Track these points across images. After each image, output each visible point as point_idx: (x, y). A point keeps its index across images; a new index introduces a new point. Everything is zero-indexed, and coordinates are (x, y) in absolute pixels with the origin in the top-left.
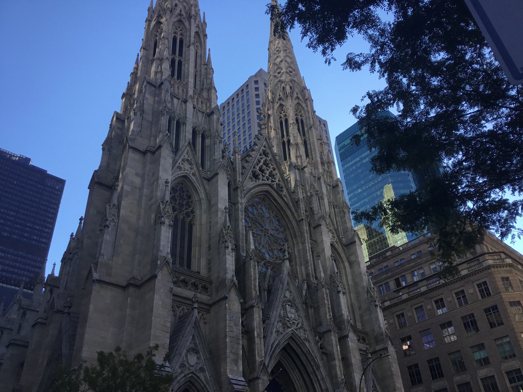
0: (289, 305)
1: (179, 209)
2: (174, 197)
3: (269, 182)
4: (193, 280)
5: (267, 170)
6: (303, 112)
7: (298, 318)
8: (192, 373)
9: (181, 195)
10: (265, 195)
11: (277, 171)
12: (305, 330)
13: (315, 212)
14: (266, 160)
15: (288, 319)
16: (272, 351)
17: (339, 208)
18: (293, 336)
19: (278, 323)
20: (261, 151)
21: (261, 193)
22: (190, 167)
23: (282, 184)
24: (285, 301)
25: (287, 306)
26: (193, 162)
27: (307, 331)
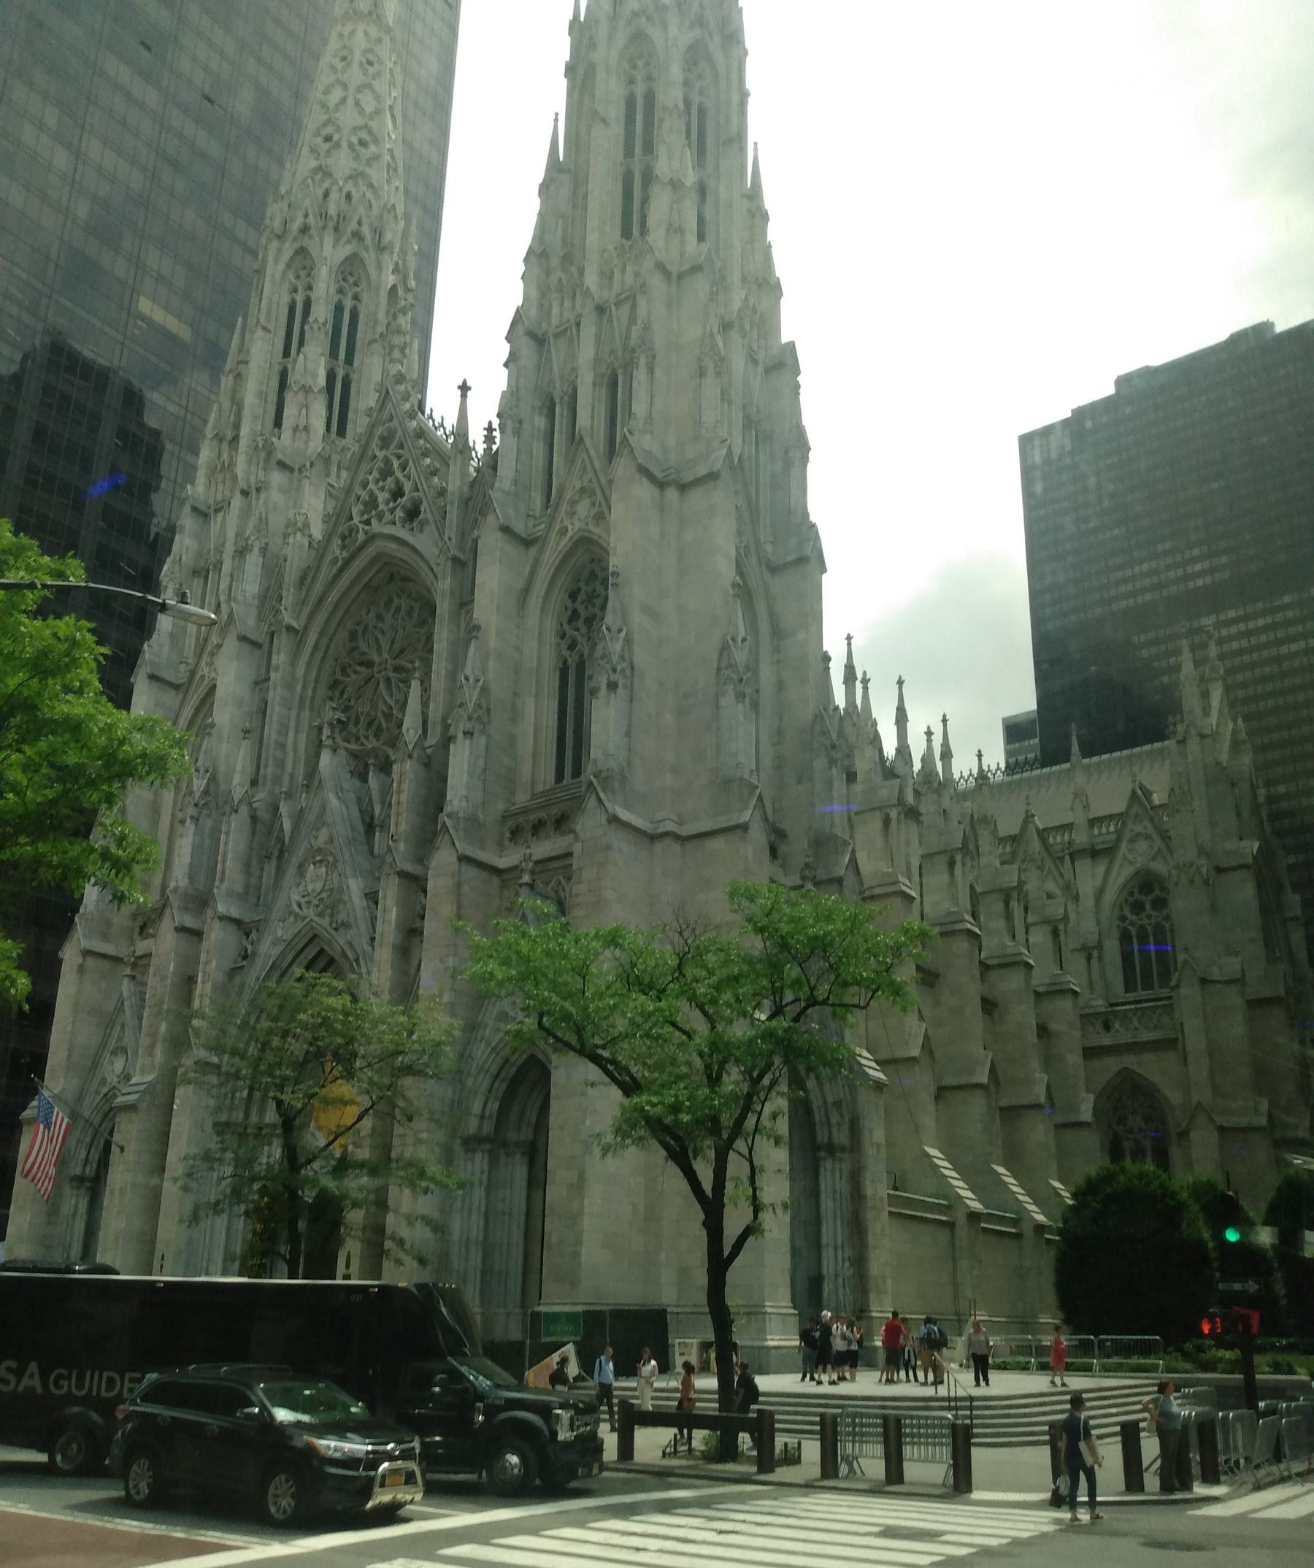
14: (387, 461)
15: (306, 899)
24: (305, 860)
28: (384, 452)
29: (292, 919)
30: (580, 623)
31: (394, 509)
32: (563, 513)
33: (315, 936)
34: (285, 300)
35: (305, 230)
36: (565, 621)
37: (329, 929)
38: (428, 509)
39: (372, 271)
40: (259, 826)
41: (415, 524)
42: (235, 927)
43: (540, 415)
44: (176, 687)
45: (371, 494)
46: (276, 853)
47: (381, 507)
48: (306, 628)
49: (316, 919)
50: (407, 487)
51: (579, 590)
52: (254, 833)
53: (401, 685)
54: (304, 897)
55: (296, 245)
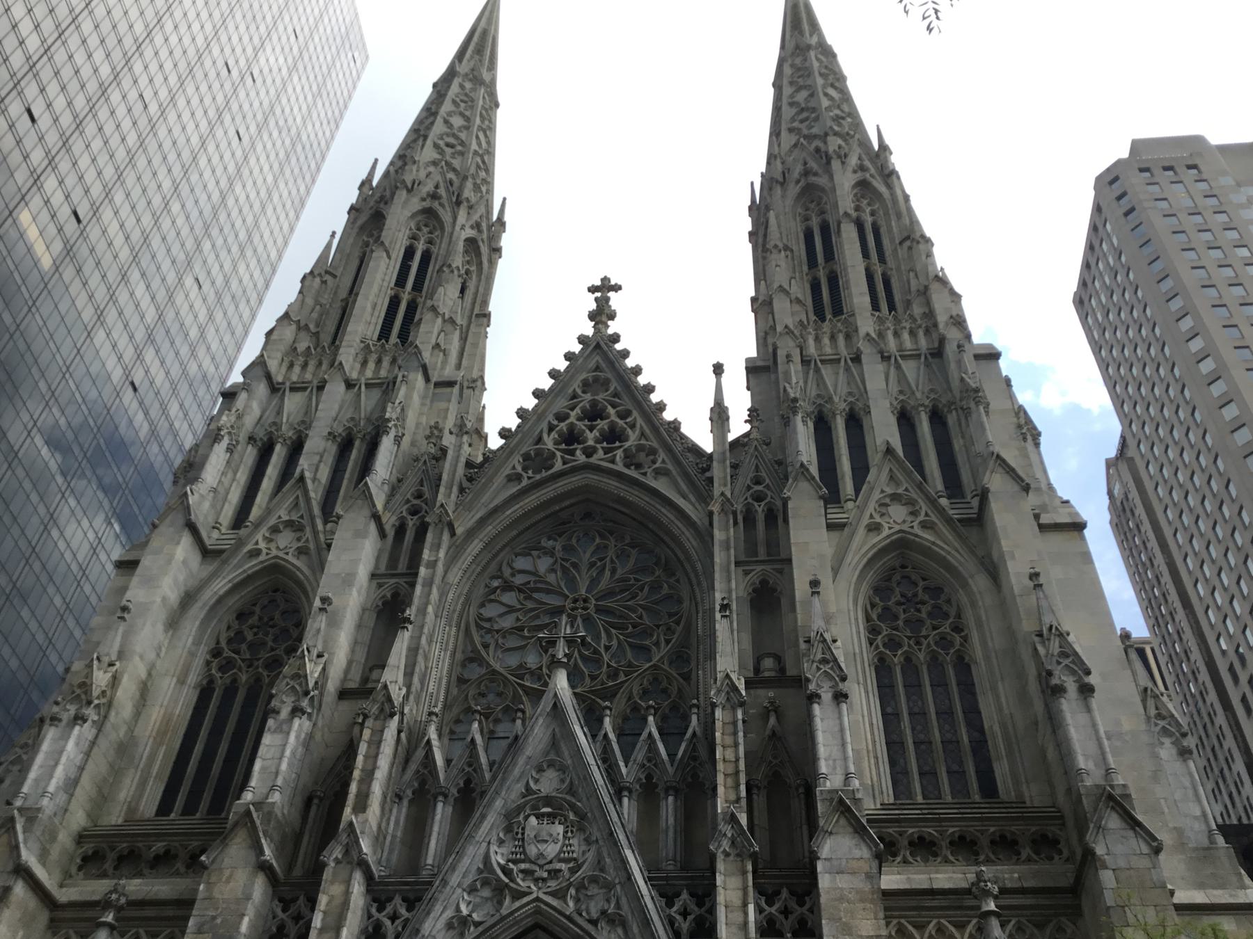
1: (243, 660)
2: (239, 633)
3: (598, 457)
4: (196, 843)
5: (591, 429)
6: (825, 199)
7: (584, 848)
9: (266, 619)
11: (635, 414)
12: (609, 886)
13: (790, 469)
14: (594, 403)
15: (523, 866)
17: (956, 409)
19: (472, 890)
20: (576, 386)
21: (567, 503)
22: (299, 534)
24: (520, 809)
25: (533, 820)
27: (614, 886)
28: (588, 397)
29: (486, 893)
30: (900, 623)
31: (610, 450)
33: (536, 926)
34: (406, 243)
35: (434, 196)
36: (875, 617)
45: (571, 427)
46: (409, 792)
49: (549, 899)
52: (396, 749)
53: (613, 631)
54: (515, 862)
55: (427, 204)
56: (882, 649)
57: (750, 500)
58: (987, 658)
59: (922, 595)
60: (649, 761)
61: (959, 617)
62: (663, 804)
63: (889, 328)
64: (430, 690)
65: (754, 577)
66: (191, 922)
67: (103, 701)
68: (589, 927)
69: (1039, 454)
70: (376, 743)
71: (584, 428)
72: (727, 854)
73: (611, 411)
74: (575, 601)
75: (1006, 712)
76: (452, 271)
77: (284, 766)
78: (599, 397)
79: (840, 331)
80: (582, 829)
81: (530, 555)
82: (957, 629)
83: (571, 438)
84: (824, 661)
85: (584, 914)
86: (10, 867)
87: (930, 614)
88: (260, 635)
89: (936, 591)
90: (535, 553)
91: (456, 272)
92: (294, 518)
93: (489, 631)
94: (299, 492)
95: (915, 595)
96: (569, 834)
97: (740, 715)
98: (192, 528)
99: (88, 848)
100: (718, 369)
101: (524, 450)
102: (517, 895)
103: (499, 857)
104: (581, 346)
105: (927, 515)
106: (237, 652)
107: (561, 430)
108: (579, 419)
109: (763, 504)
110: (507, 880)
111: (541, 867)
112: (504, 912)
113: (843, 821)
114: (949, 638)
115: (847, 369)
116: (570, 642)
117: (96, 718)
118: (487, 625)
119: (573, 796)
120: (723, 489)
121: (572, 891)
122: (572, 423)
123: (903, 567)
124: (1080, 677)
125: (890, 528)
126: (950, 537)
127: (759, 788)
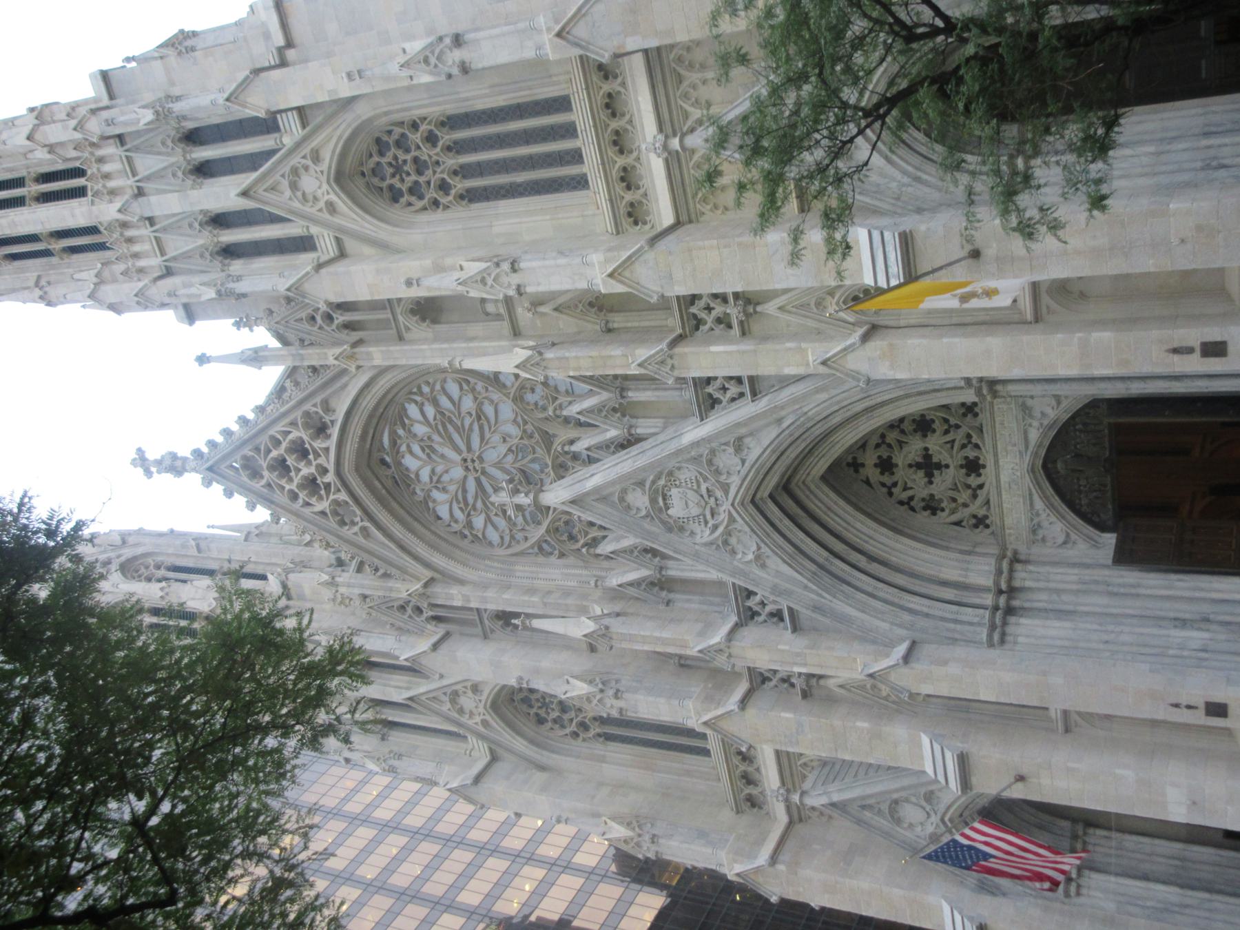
0: (667, 508)
1: (577, 716)
8: (942, 820)
9: (540, 704)
10: (369, 466)
11: (272, 432)
14: (271, 468)
15: (709, 517)
16: (820, 591)
18: (749, 498)
19: (734, 552)
20: (258, 485)
21: (377, 483)
22: (460, 693)
23: (298, 414)
24: (664, 523)
25: (670, 512)
26: (449, 691)
28: (266, 473)
30: (422, 179)
32: (313, 210)
33: (753, 501)
36: (420, 204)
37: (743, 473)
38: (314, 402)
39: (139, 551)
40: (631, 610)
41: (327, 419)
42: (742, 629)
43: (229, 265)
44: (494, 758)
45: (301, 486)
46: (664, 594)
47: (312, 470)
48: (427, 565)
50: (295, 434)
51: (391, 187)
52: (632, 614)
54: (706, 523)
56: (450, 198)
57: (334, 327)
58: (439, 104)
59: (389, 157)
60: (600, 411)
61: (403, 123)
62: (635, 399)
63: (104, 186)
64: (575, 584)
65: (412, 322)
66: (791, 750)
67: (635, 824)
68: (747, 465)
69: (204, 32)
70: (631, 638)
71: (299, 477)
72: (673, 367)
73: (274, 454)
74: (467, 469)
75: (487, 91)
76: (167, 594)
77: (662, 700)
78: (265, 465)
79: (122, 235)
80: (670, 474)
81: (434, 509)
82: (415, 126)
83: (311, 484)
84: (483, 281)
85: (738, 468)
86: (771, 869)
87: (407, 151)
88: (553, 706)
89: (381, 146)
90: (431, 505)
91: (167, 590)
92: (446, 699)
93: (512, 537)
94: (423, 698)
95: (390, 164)
96: (677, 483)
97: (549, 355)
98: (478, 779)
99: (746, 806)
100: (202, 359)
101: (336, 526)
102: (732, 520)
103: (704, 535)
104: (214, 483)
105: (304, 157)
106: (571, 720)
107: (306, 495)
108: (291, 480)
109: (334, 315)
110: (721, 529)
111: (707, 503)
112: (747, 529)
113: (627, 274)
114: (425, 134)
115: (164, 230)
116: (516, 492)
117: (649, 825)
118: (507, 539)
119: (645, 481)
120: (331, 358)
121: (723, 478)
122: (297, 487)
123: (363, 174)
124: (446, 47)
125: (328, 193)
126: (323, 136)
127: (607, 322)
